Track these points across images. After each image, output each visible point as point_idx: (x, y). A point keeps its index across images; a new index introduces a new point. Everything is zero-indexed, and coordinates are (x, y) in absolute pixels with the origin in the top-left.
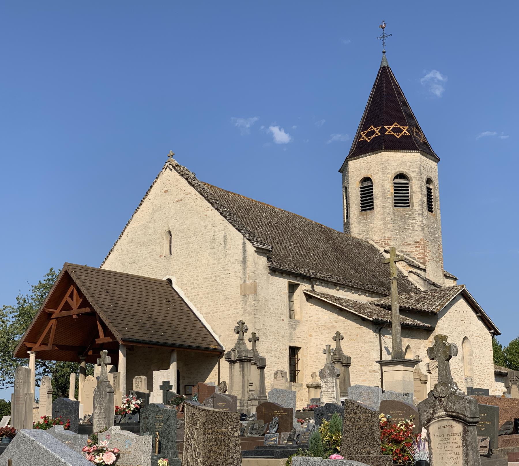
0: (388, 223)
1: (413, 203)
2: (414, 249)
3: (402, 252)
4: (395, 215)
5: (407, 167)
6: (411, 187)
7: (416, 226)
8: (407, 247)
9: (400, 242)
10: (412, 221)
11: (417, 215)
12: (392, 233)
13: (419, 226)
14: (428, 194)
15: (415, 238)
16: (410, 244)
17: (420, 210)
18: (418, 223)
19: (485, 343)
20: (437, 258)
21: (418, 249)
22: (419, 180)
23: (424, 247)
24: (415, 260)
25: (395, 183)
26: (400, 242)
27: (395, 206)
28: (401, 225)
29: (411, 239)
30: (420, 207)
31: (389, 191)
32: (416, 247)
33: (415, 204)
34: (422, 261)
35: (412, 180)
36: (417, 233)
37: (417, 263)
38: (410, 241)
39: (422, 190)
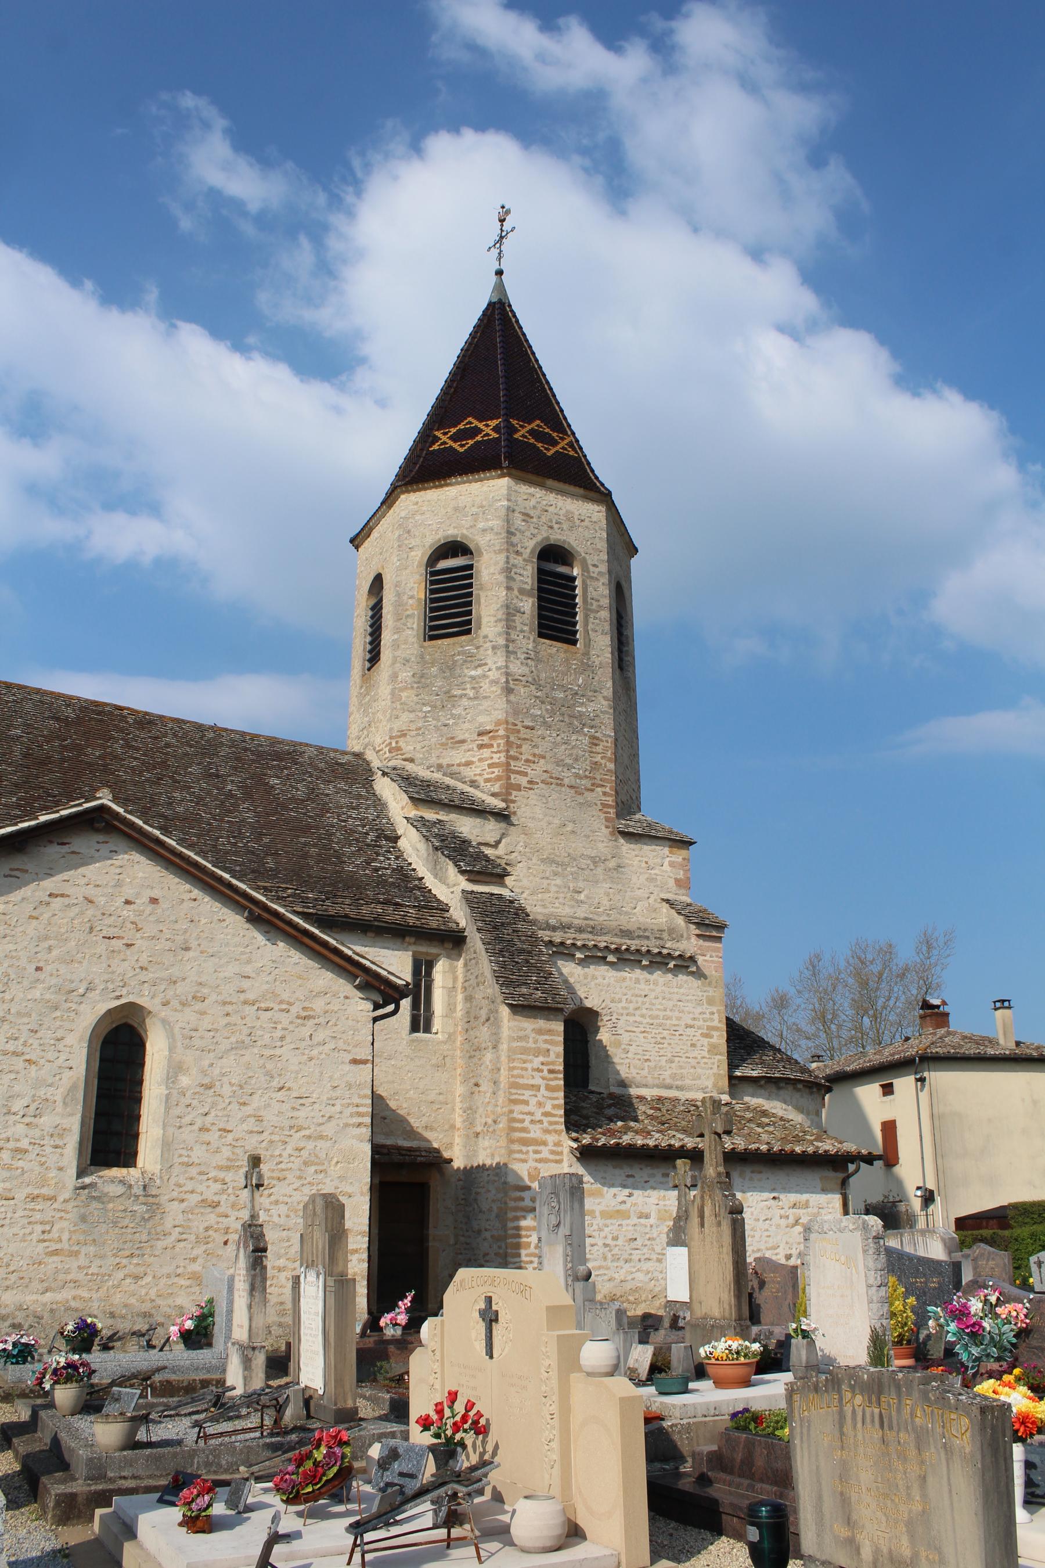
0: (402, 690)
1: (479, 618)
2: (475, 756)
3: (440, 767)
4: (426, 663)
5: (467, 522)
6: (479, 572)
7: (485, 685)
8: (454, 752)
9: (433, 738)
10: (473, 673)
11: (490, 652)
12: (412, 716)
13: (495, 682)
14: (540, 589)
15: (481, 719)
16: (463, 741)
17: (500, 634)
18: (493, 675)
19: (306, 1032)
20: (577, 776)
21: (486, 753)
22: (500, 551)
23: (509, 744)
24: (477, 787)
25: (433, 574)
26: (433, 738)
27: (432, 638)
28: (440, 688)
29: (466, 726)
30: (500, 628)
31: (412, 597)
32: (481, 747)
33: (484, 621)
34: (496, 788)
35: (480, 554)
36: (486, 704)
37: (484, 797)
38: (465, 730)
39: (509, 578)
